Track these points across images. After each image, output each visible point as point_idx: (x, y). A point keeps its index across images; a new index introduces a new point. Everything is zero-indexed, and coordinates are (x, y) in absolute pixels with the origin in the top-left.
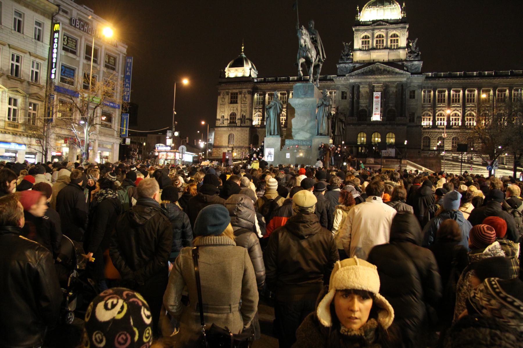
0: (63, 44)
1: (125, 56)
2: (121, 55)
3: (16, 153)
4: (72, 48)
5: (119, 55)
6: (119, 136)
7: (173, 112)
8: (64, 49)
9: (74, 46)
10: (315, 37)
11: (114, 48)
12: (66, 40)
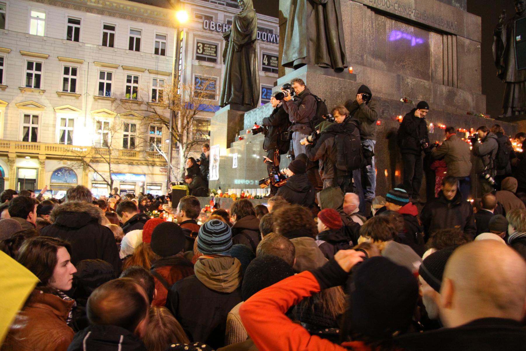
0: (197, 53)
3: (135, 185)
4: (210, 55)
8: (198, 58)
9: (213, 52)
11: (275, 45)
12: (201, 48)
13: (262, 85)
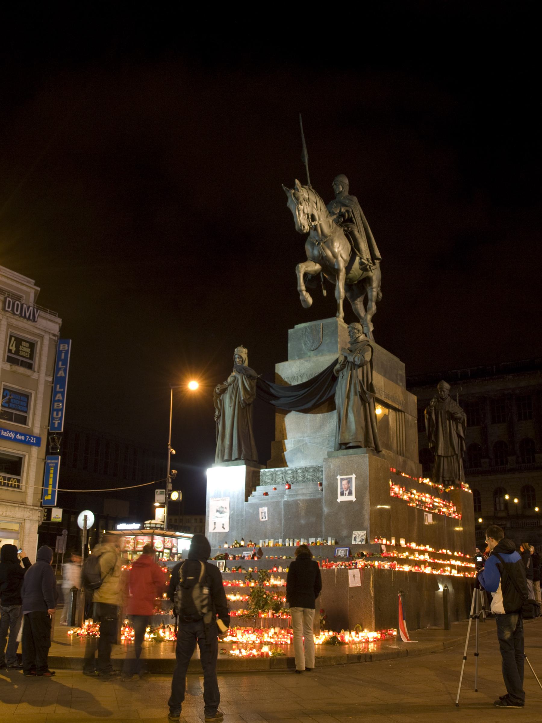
1: (56, 338)
2: (47, 337)
5: (42, 337)
6: (39, 504)
7: (167, 450)
10: (348, 211)
11: (30, 322)
13: (4, 385)
